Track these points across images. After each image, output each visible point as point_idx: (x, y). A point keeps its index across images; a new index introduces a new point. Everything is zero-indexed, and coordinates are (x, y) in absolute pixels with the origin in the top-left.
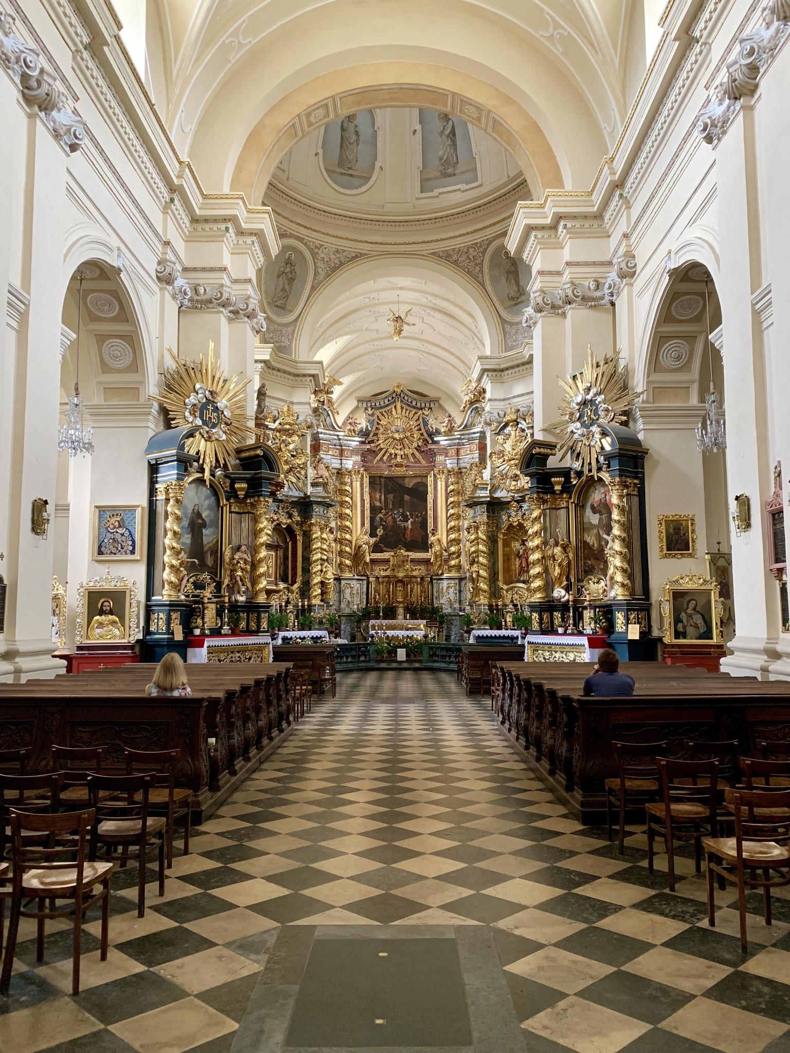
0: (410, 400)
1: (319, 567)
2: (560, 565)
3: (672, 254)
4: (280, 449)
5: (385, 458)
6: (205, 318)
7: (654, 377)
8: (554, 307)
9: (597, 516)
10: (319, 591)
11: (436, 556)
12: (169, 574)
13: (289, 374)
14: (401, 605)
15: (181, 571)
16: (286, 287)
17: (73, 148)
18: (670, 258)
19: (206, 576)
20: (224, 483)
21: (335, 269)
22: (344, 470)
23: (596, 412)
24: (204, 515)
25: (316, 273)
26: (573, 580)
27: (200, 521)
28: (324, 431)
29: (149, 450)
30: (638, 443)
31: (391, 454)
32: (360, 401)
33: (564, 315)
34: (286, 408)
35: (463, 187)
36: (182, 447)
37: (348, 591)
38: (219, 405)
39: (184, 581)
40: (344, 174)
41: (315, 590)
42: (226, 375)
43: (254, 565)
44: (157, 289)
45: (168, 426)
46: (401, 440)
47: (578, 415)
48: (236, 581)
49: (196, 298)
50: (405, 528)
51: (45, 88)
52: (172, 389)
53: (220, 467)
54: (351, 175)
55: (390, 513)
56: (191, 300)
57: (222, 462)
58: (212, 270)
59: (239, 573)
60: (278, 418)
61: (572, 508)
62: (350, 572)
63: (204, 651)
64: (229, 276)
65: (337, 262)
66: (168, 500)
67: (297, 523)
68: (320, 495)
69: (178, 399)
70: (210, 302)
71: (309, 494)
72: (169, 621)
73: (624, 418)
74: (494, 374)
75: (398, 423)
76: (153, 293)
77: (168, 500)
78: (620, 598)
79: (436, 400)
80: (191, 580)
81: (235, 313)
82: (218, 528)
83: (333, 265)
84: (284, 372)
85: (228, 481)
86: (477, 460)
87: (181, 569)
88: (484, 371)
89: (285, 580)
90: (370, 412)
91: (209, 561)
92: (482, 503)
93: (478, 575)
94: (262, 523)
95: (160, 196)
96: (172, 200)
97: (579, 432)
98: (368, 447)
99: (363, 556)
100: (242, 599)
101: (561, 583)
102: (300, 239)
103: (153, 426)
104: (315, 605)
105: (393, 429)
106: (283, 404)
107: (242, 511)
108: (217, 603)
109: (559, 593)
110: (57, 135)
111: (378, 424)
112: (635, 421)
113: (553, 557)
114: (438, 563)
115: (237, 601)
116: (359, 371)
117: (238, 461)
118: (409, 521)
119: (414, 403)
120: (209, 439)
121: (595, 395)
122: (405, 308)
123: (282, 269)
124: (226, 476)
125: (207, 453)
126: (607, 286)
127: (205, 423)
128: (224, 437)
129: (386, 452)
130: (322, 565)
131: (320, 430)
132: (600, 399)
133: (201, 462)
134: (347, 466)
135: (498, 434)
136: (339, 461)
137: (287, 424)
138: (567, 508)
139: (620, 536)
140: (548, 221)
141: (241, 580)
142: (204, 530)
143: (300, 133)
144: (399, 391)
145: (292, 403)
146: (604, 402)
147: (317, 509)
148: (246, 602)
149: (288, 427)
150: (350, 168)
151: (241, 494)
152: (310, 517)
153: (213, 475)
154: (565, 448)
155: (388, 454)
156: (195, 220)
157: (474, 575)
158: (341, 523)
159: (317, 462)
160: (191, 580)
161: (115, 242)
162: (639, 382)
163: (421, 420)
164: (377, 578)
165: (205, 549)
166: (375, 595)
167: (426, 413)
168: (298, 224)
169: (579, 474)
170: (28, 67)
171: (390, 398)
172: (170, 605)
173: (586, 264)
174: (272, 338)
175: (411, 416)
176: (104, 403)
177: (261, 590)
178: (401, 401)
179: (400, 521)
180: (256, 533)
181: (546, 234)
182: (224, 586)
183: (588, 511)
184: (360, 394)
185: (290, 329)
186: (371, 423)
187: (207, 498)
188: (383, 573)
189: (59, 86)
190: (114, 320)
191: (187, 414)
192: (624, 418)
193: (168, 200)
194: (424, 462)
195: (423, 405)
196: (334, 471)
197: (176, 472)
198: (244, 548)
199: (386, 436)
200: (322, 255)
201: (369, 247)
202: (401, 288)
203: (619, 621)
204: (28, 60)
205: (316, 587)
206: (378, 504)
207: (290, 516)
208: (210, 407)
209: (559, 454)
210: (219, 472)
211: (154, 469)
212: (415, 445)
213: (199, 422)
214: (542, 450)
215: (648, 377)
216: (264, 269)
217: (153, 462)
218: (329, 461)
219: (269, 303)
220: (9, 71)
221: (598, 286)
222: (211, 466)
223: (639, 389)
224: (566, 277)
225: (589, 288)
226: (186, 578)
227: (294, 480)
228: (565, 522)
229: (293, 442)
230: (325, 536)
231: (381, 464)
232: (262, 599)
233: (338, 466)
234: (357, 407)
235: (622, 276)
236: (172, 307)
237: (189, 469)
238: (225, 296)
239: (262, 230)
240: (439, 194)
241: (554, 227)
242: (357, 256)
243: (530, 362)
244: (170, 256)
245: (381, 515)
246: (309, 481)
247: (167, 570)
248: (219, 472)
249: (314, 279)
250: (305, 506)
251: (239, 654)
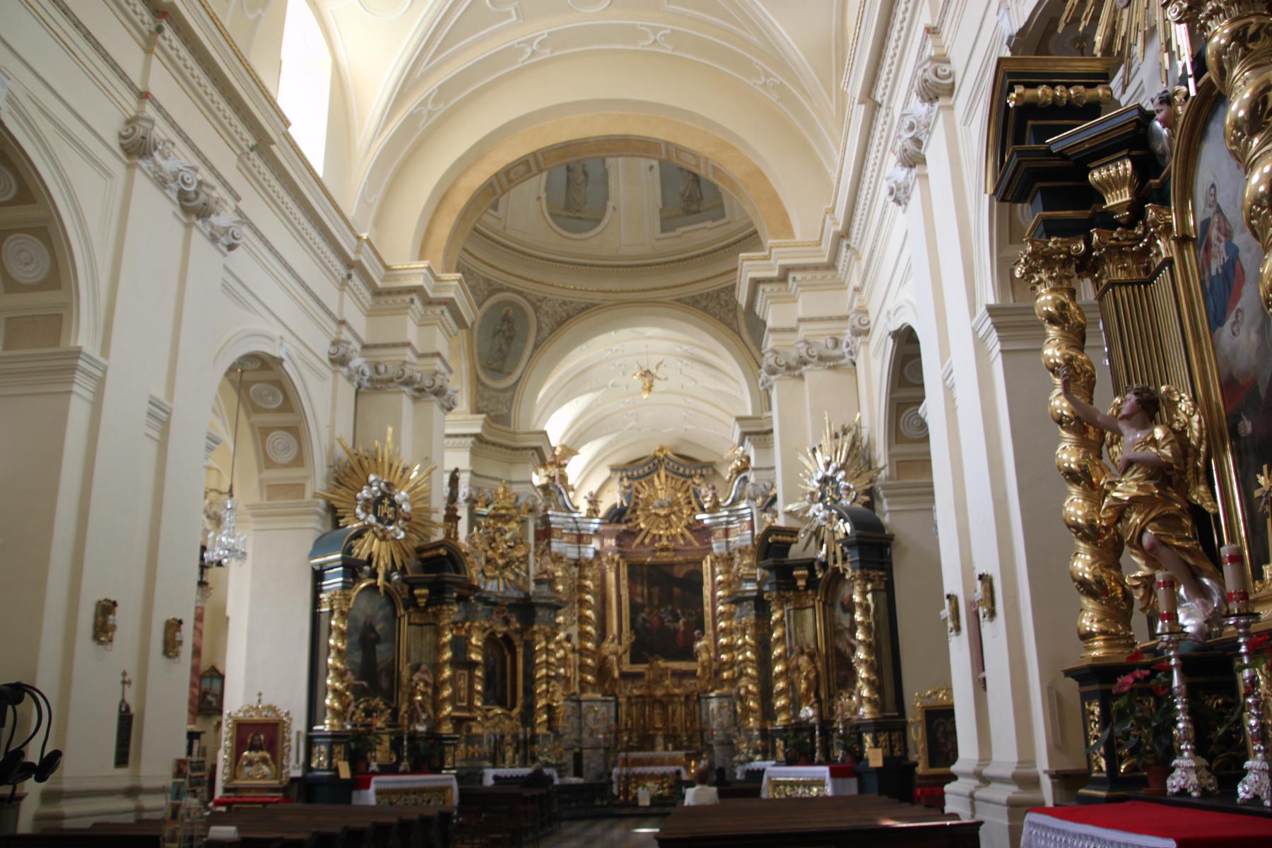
0: (676, 467)
1: (544, 687)
2: (806, 678)
3: (891, 315)
4: (494, 540)
5: (647, 541)
6: (386, 399)
7: (898, 449)
8: (789, 368)
9: (848, 616)
10: (545, 717)
11: (704, 668)
12: (331, 700)
13: (507, 447)
14: (660, 733)
15: (347, 697)
16: (505, 348)
17: (231, 247)
18: (889, 319)
19: (378, 702)
20: (402, 589)
21: (560, 323)
22: (583, 562)
23: (837, 491)
24: (379, 627)
25: (539, 330)
26: (823, 696)
27: (373, 636)
28: (555, 513)
29: (313, 555)
30: (879, 527)
31: (654, 536)
32: (614, 469)
33: (801, 377)
34: (501, 490)
35: (709, 224)
36: (348, 551)
37: (591, 716)
38: (396, 497)
39: (352, 708)
40: (571, 217)
41: (540, 716)
42: (406, 461)
43: (437, 687)
44: (329, 373)
45: (336, 526)
46: (667, 516)
47: (819, 494)
48: (415, 709)
49: (376, 377)
50: (676, 631)
51: (202, 197)
52: (341, 484)
53: (396, 570)
54: (579, 218)
55: (655, 612)
56: (370, 380)
57: (399, 565)
58: (394, 345)
59: (419, 698)
60: (491, 502)
61: (819, 606)
62: (594, 691)
63: (372, 790)
64: (414, 351)
65: (564, 315)
66: (332, 612)
67: (517, 631)
68: (545, 594)
69: (349, 494)
70: (391, 380)
71: (531, 594)
72: (330, 756)
73: (867, 498)
74: (757, 437)
75: (662, 495)
76: (322, 377)
77: (332, 612)
78: (867, 716)
79: (710, 465)
80: (361, 706)
81: (421, 390)
82: (394, 642)
83: (559, 319)
84: (501, 446)
85: (406, 587)
86: (749, 543)
87: (348, 693)
88: (744, 435)
89: (502, 703)
90: (626, 483)
91: (384, 683)
92: (747, 599)
93: (748, 692)
94: (446, 636)
95: (336, 273)
96: (349, 276)
97: (822, 514)
98: (624, 527)
99: (610, 671)
100: (421, 728)
101: (809, 700)
102: (520, 293)
103: (313, 527)
104: (538, 736)
105: (656, 503)
106: (497, 483)
107: (423, 622)
108: (391, 734)
109: (807, 712)
110: (214, 239)
111: (637, 498)
112: (881, 501)
113: (798, 668)
114: (707, 677)
115: (416, 732)
116: (607, 434)
117: (419, 563)
118: (681, 622)
119: (681, 470)
120: (384, 539)
121: (837, 470)
122: (656, 359)
123: (498, 327)
124: (405, 581)
125: (381, 555)
126: (844, 345)
127: (379, 520)
128: (402, 535)
129: (648, 533)
130: (548, 683)
131: (550, 512)
132: (840, 475)
133: (374, 564)
134: (587, 556)
135: (765, 511)
136: (576, 550)
137: (502, 508)
138: (813, 607)
139: (864, 641)
140: (775, 274)
141: (421, 706)
143: (499, 191)
144: (662, 455)
145: (511, 482)
146: (845, 479)
147: (541, 613)
148: (427, 732)
149: (503, 512)
150: (578, 211)
151: (422, 602)
152: (532, 624)
153: (388, 578)
154: (809, 534)
155: (650, 536)
156: (377, 293)
157: (742, 692)
158: (581, 628)
159: (544, 551)
160: (361, 706)
161: (277, 331)
162: (881, 455)
163: (691, 491)
164: (629, 698)
166: (627, 721)
167: (697, 481)
168: (518, 276)
169: (824, 565)
170: (184, 183)
171: (651, 465)
172: (332, 737)
173: (821, 320)
174: (486, 407)
175: (678, 485)
176: (265, 502)
177: (445, 718)
178: (666, 469)
179: (669, 621)
180: (439, 649)
181: (775, 287)
182: (401, 713)
183: (838, 611)
184: (613, 460)
185: (508, 395)
186: (628, 497)
188: (636, 692)
189: (220, 192)
190: (279, 410)
191: (358, 510)
192: (867, 498)
193: (345, 276)
194: (697, 544)
195: (693, 472)
196: (572, 562)
197: (341, 579)
198: (424, 667)
199: (647, 513)
200: (546, 308)
201: (600, 296)
202: (649, 338)
203: (867, 745)
204: (185, 178)
205: (540, 712)
206: (639, 600)
207: (507, 622)
208: (386, 501)
209: (802, 543)
210: (395, 577)
211: (318, 576)
212: (684, 523)
213: (372, 519)
214: (780, 538)
215: (890, 447)
216: (476, 327)
217: (317, 568)
218: (563, 550)
219: (483, 367)
220: (168, 192)
221: (837, 343)
222: (386, 570)
223: (881, 464)
224: (801, 335)
225: (827, 347)
226: (353, 704)
227: (512, 577)
228: (812, 624)
229: (511, 530)
230: (552, 646)
231: (642, 549)
232: (447, 729)
233: (575, 556)
234: (609, 479)
235: (857, 333)
236: (347, 391)
237: (360, 574)
238: (408, 373)
239: (452, 300)
240: (683, 233)
241: (783, 279)
242: (587, 308)
243: (771, 431)
244: (346, 335)
245: (643, 615)
246: (532, 578)
247: (330, 696)
248: (395, 577)
249: (537, 336)
250: (526, 609)
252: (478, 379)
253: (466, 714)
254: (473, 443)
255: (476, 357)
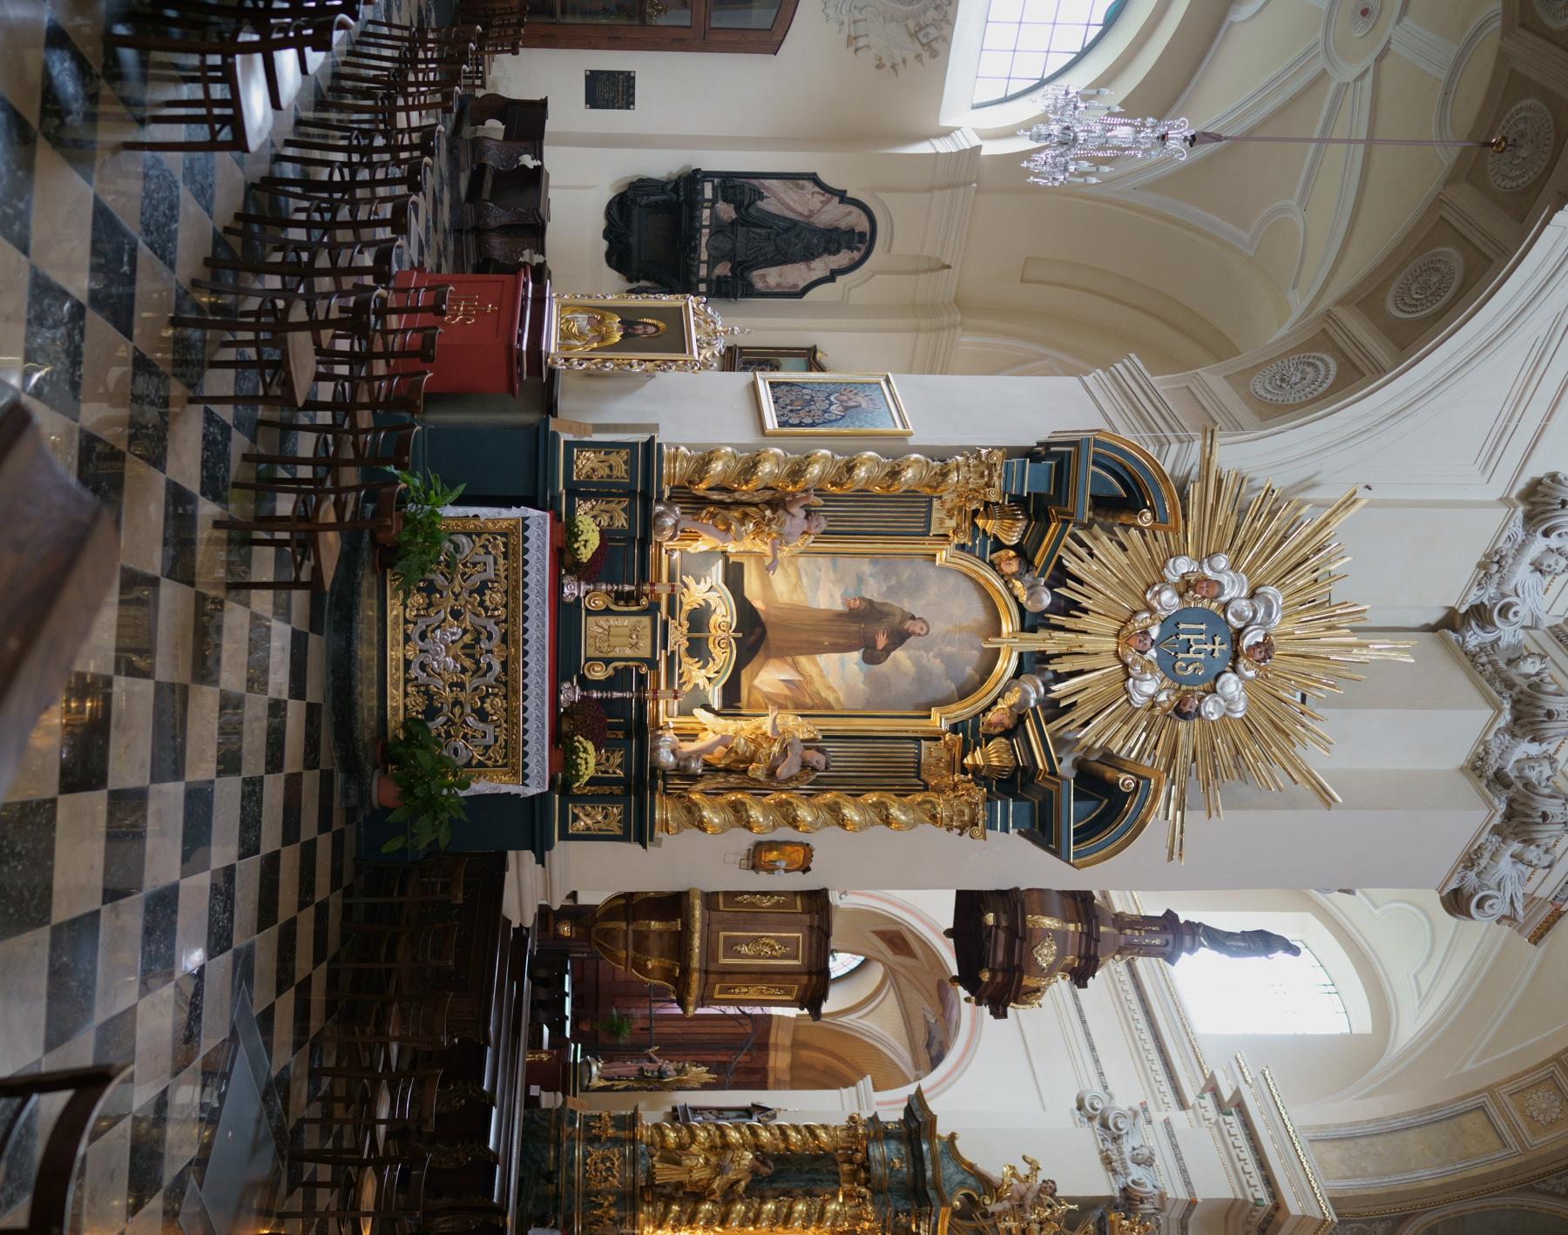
27: (882, 642)
82: (863, 710)
142: (856, 656)
165: (803, 660)
187: (948, 660)
251: (497, 667)
252: (1402, 1220)
253: (695, 963)
254: (1258, 1202)
255: (1451, 1210)
